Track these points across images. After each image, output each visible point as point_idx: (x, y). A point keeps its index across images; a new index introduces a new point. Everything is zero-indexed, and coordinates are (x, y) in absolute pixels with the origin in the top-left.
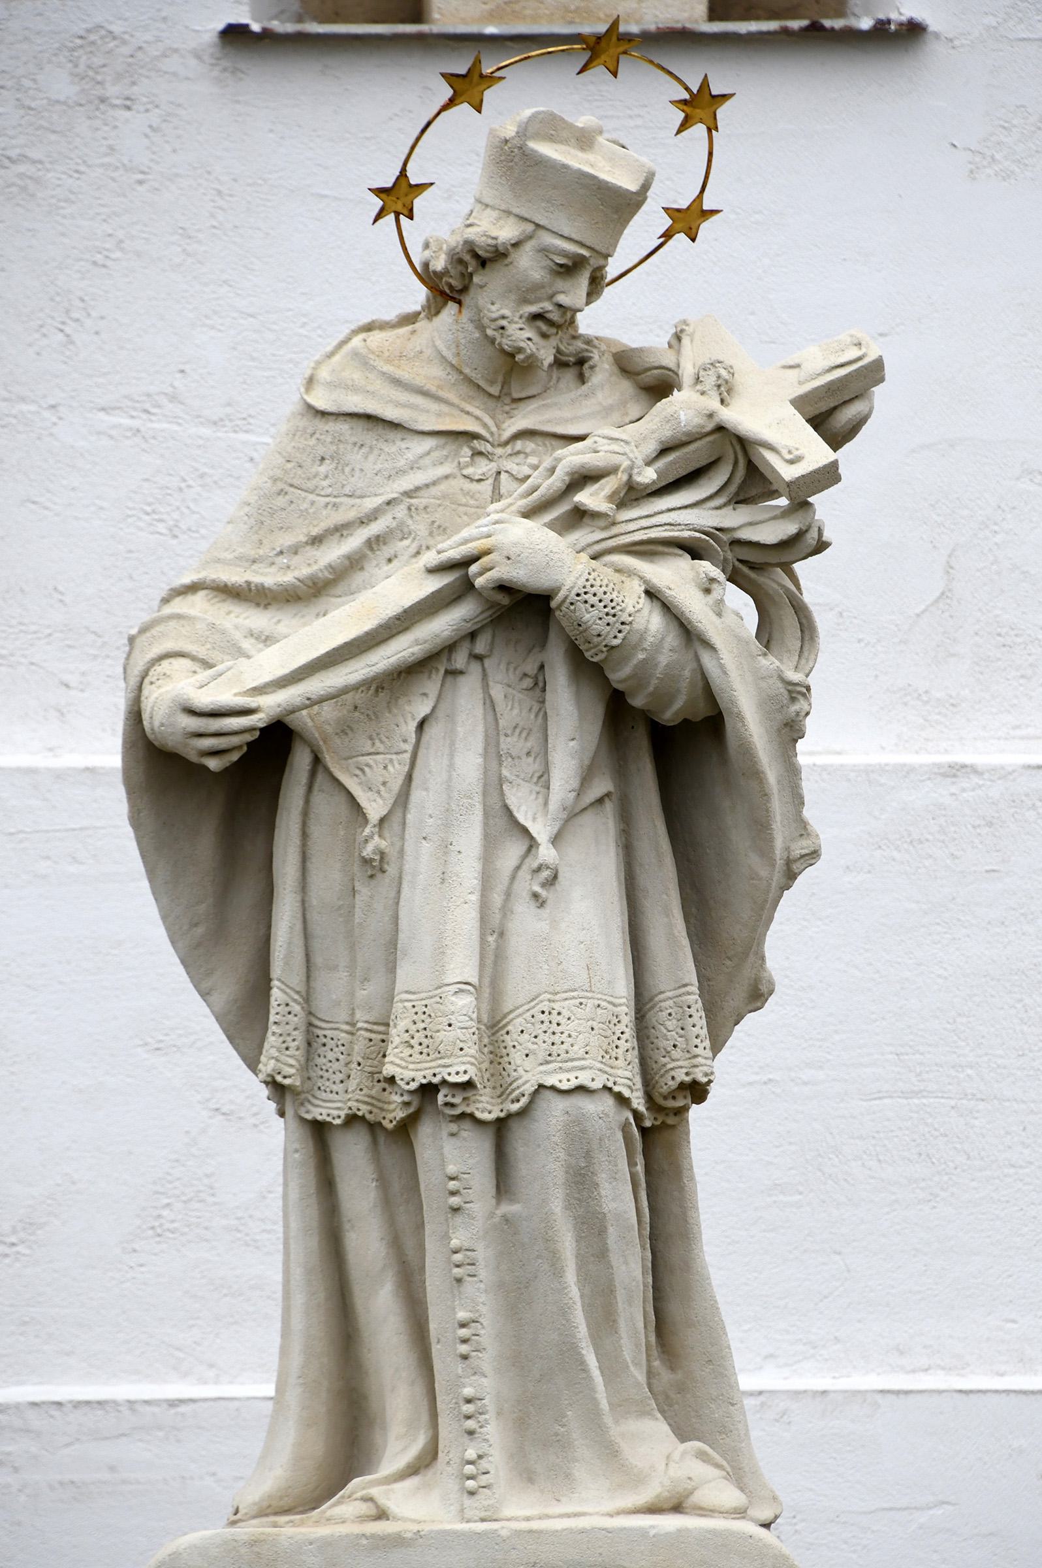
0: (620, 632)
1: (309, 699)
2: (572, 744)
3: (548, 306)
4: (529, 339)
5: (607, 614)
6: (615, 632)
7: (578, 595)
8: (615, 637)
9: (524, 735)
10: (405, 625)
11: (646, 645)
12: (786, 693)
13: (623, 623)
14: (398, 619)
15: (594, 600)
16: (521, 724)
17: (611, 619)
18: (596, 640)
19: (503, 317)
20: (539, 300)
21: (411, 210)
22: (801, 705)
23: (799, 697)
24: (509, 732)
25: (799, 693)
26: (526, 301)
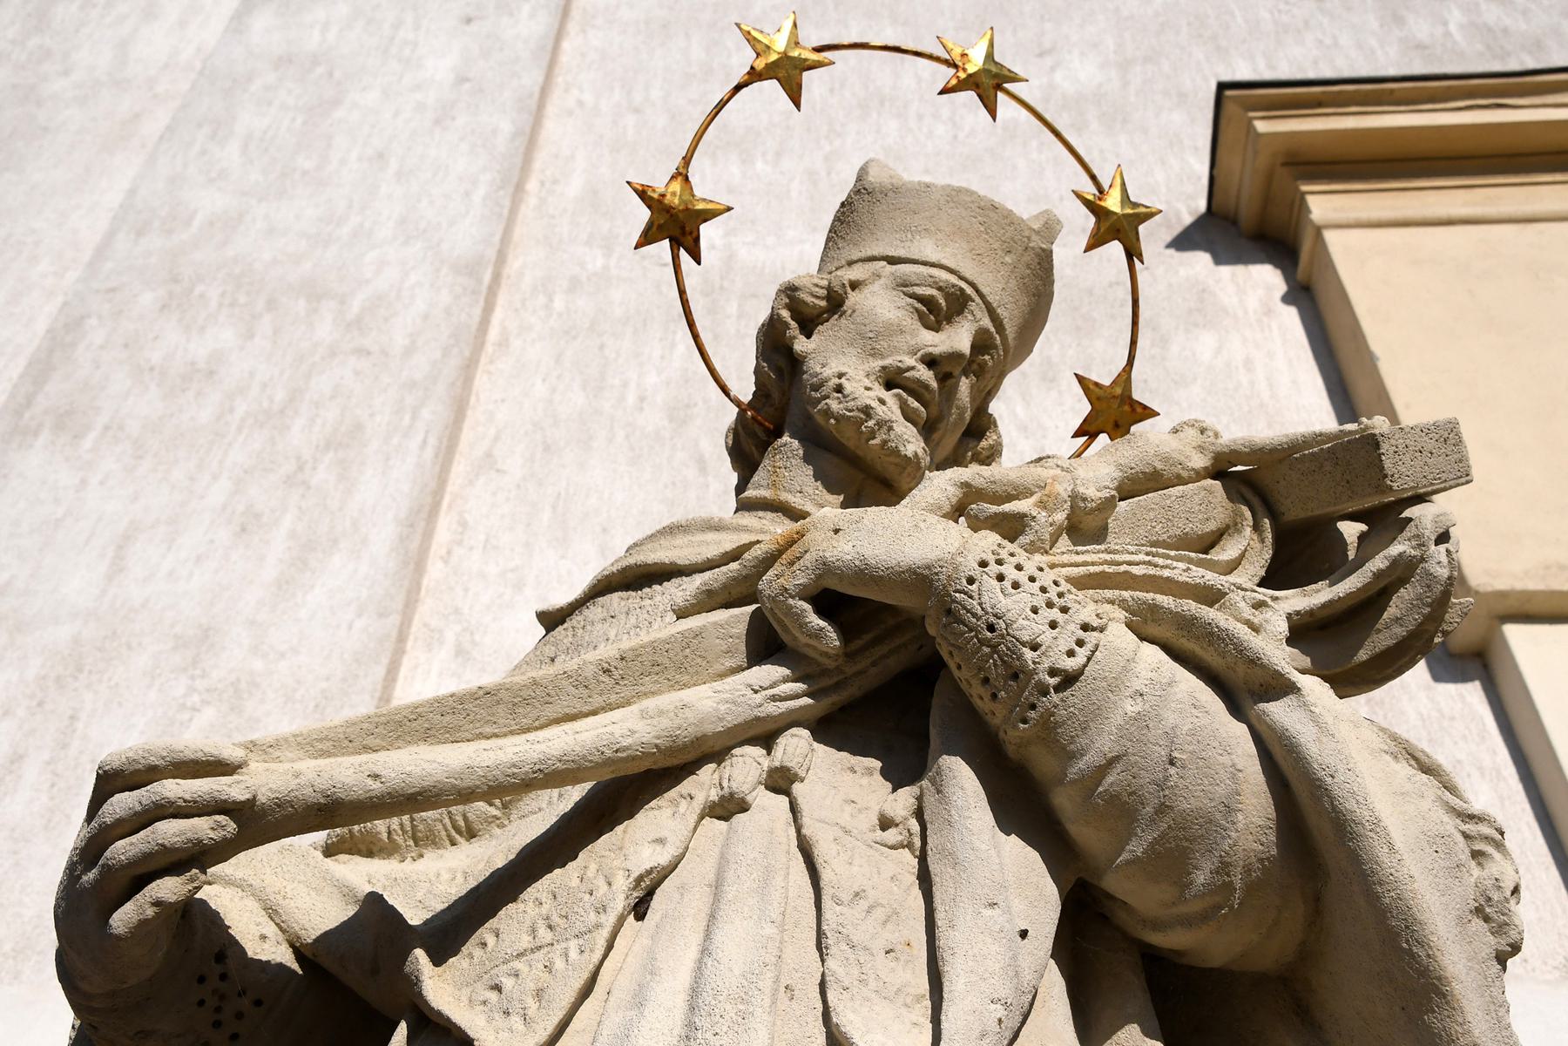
0: (1080, 643)
1: (376, 777)
2: (988, 912)
3: (910, 361)
4: (882, 402)
5: (1050, 605)
6: (1067, 642)
7: (983, 564)
8: (1071, 653)
9: (879, 913)
10: (627, 692)
11: (1137, 685)
12: (1460, 839)
13: (1085, 627)
14: (606, 671)
15: (1022, 577)
16: (871, 893)
17: (1055, 614)
18: (1029, 654)
19: (840, 376)
20: (895, 350)
21: (697, 240)
22: (1498, 866)
23: (1490, 849)
24: (845, 897)
25: (1487, 839)
26: (875, 354)
